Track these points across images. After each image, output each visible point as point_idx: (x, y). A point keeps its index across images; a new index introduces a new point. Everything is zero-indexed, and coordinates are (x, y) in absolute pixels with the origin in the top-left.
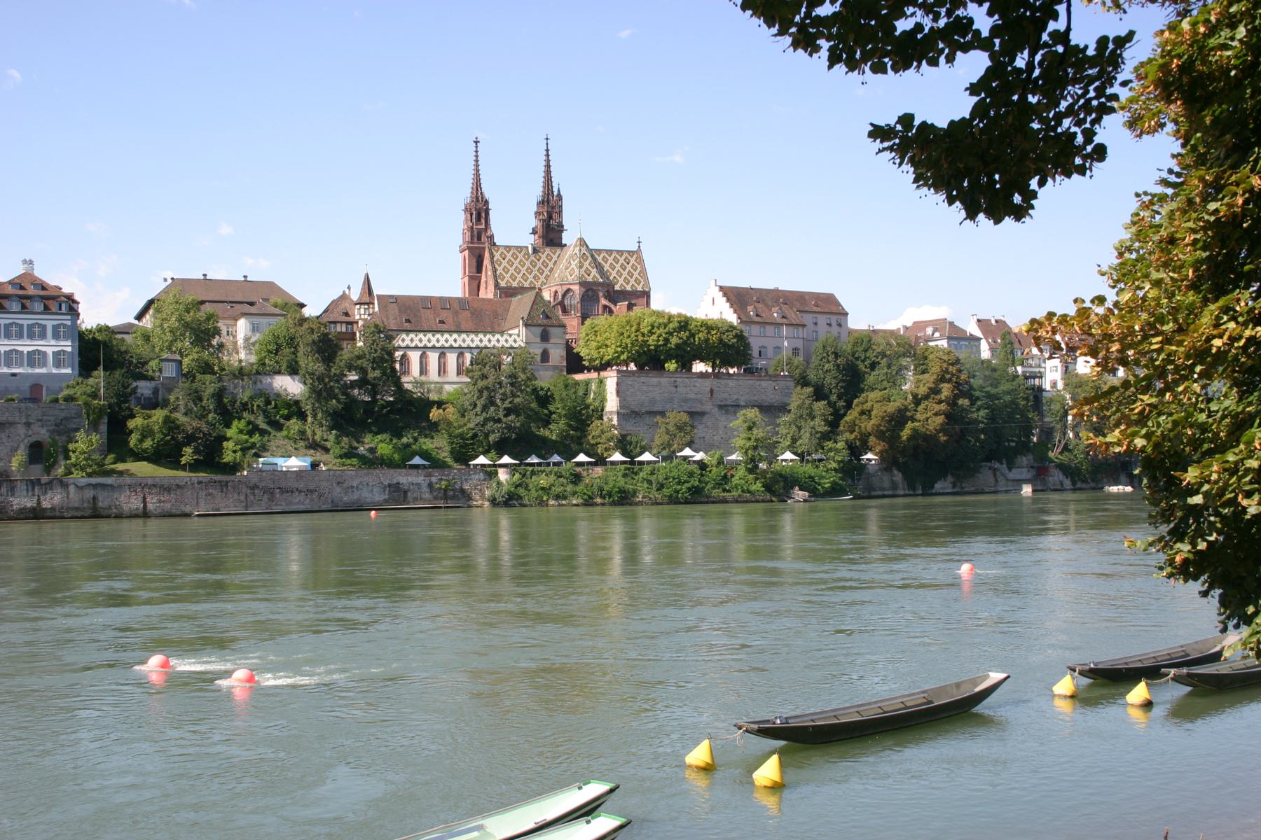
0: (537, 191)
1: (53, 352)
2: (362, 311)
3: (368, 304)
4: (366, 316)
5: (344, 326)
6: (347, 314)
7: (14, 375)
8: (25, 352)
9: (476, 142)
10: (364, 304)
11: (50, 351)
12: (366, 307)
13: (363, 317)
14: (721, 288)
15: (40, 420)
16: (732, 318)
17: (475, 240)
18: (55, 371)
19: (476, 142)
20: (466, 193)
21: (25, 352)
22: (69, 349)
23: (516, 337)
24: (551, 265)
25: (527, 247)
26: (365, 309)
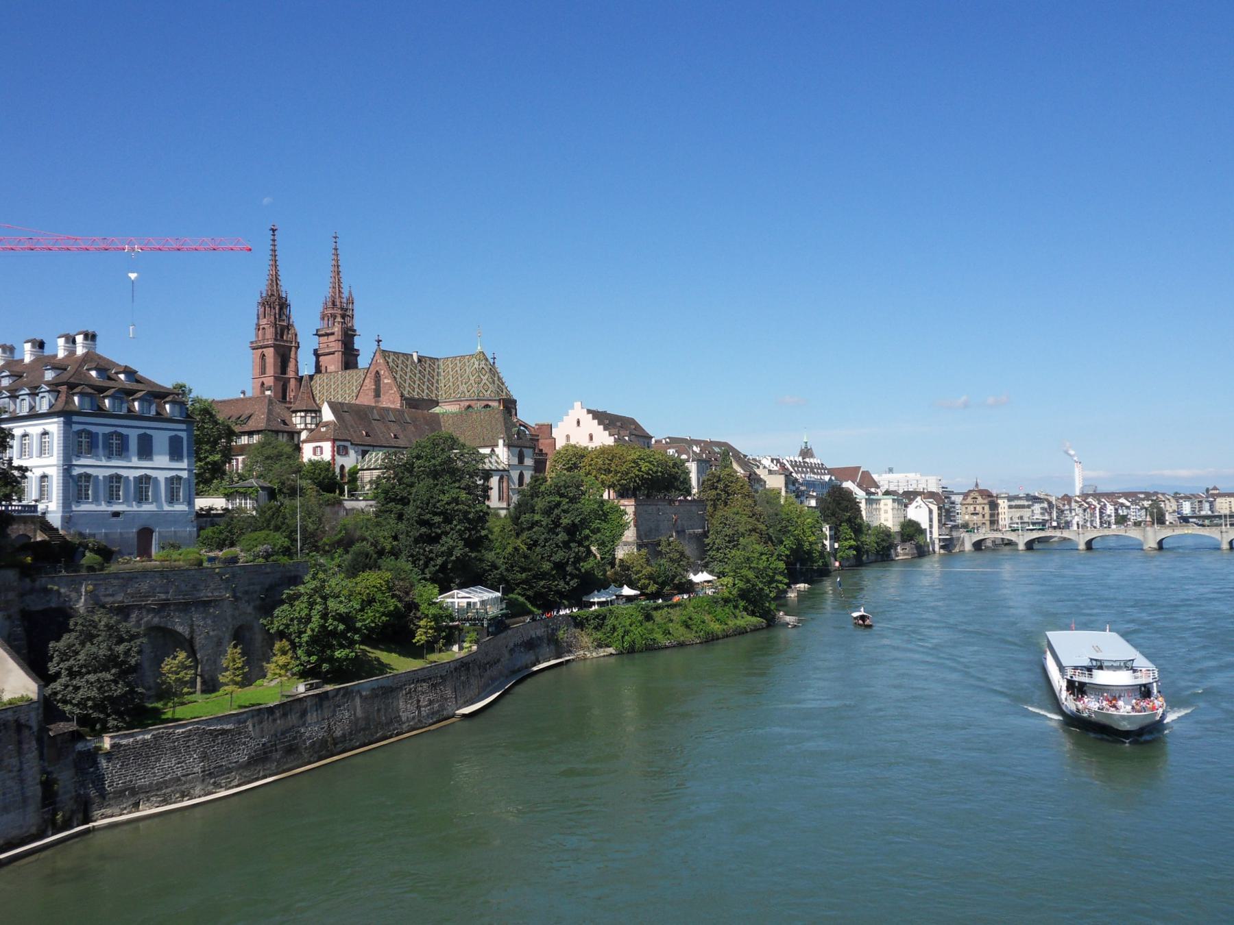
0: (326, 291)
1: (166, 478)
2: (309, 420)
3: (315, 411)
4: (313, 426)
5: (285, 435)
6: (284, 422)
7: (116, 514)
8: (131, 478)
9: (274, 230)
10: (311, 411)
11: (162, 476)
12: (313, 415)
13: (309, 426)
14: (589, 411)
15: (246, 592)
16: (604, 439)
17: (279, 338)
18: (167, 508)
19: (274, 230)
20: (261, 286)
21: (131, 478)
22: (184, 474)
23: (495, 458)
24: (436, 377)
25: (412, 355)
26: (312, 417)
